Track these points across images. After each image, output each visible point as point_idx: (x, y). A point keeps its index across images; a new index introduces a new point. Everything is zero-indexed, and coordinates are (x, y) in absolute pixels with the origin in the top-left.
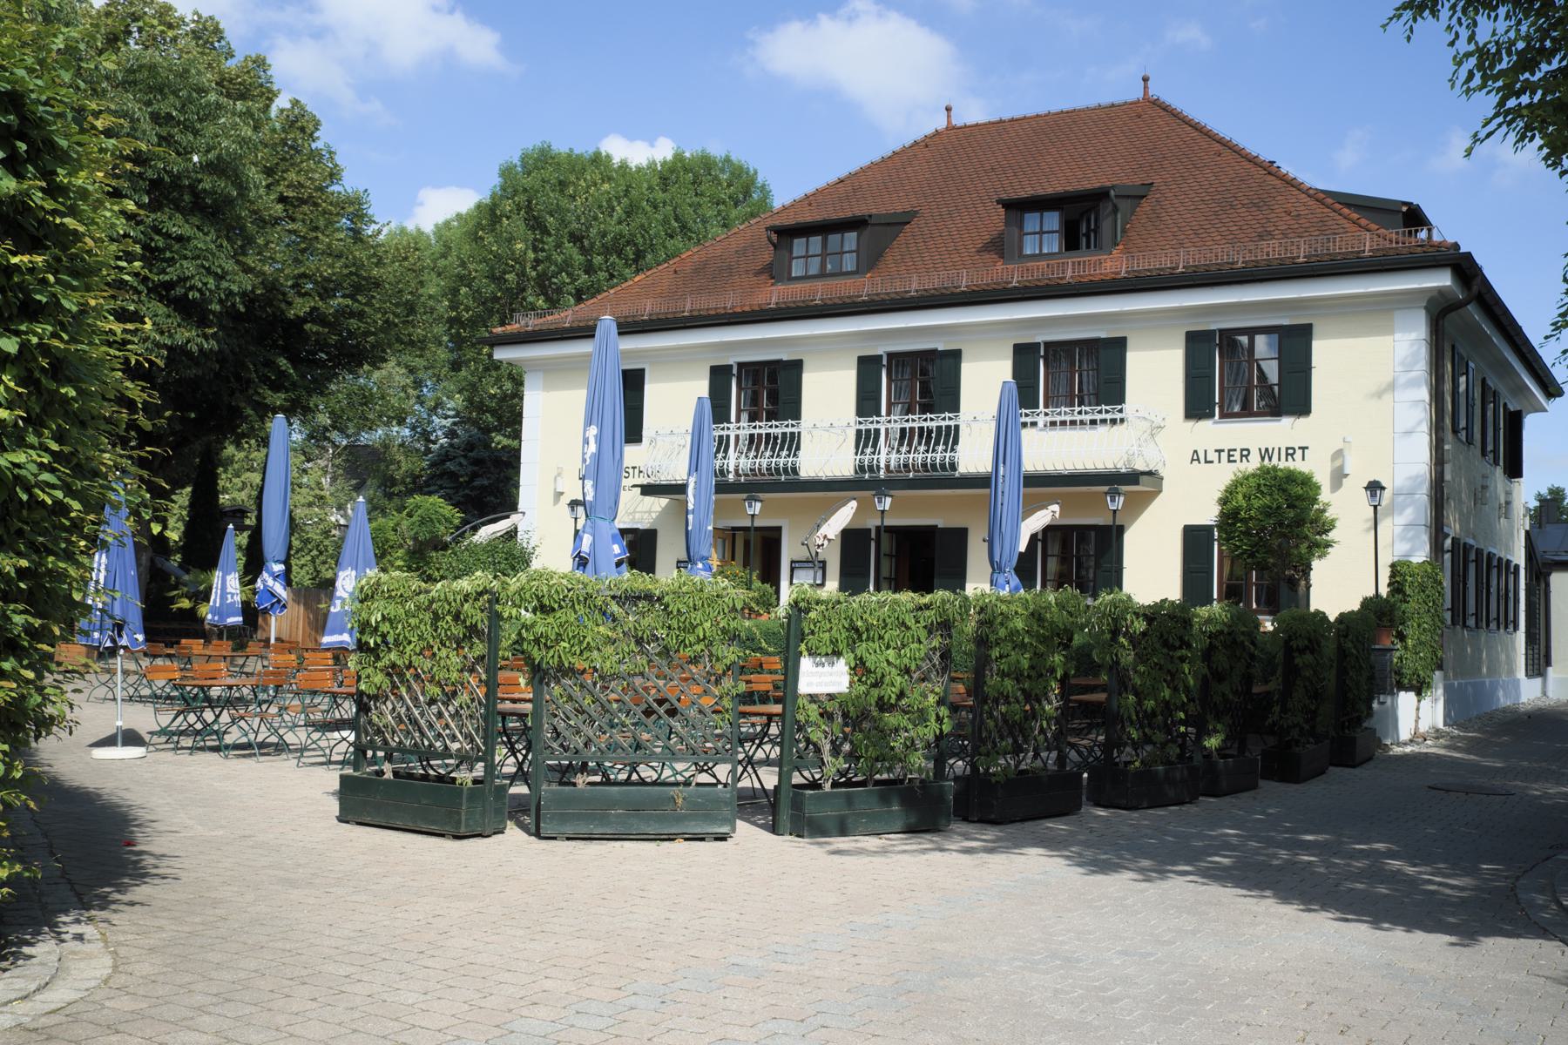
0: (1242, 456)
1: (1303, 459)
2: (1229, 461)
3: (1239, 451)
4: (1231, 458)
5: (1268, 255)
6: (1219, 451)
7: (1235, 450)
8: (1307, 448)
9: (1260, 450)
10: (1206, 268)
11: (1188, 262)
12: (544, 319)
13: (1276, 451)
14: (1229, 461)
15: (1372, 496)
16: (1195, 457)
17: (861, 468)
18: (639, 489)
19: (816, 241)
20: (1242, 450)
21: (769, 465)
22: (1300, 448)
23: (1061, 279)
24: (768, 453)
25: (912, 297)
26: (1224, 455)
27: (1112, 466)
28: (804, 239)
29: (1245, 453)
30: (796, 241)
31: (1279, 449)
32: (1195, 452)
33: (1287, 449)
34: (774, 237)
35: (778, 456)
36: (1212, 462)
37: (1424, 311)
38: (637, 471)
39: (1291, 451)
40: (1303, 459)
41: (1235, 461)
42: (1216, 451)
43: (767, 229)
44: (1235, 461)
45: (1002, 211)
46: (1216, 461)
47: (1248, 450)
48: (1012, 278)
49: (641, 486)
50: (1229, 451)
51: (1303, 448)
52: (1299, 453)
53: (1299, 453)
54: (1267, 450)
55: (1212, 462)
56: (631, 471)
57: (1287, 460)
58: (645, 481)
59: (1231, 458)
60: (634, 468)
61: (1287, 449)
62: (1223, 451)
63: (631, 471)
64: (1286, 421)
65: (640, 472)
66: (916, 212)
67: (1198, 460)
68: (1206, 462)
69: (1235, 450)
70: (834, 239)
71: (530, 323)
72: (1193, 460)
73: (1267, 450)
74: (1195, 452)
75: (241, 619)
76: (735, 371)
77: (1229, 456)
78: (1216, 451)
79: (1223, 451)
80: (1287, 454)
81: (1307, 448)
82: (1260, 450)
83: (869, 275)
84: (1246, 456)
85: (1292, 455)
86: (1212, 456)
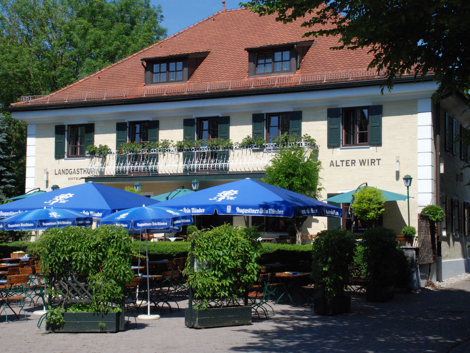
0: (352, 163)
1: (379, 164)
2: (347, 165)
3: (351, 161)
4: (347, 164)
5: (363, 75)
6: (342, 161)
7: (349, 161)
8: (380, 159)
9: (360, 160)
10: (336, 81)
11: (328, 78)
12: (36, 99)
13: (367, 161)
14: (347, 165)
15: (406, 182)
16: (332, 164)
17: (185, 170)
18: (84, 179)
19: (164, 66)
20: (352, 161)
21: (144, 168)
22: (377, 159)
23: (273, 85)
24: (122, 164)
25: (207, 93)
26: (344, 163)
27: (248, 170)
28: (175, 63)
29: (353, 162)
30: (155, 66)
31: (368, 160)
32: (332, 161)
33: (372, 160)
34: (145, 64)
35: (202, 162)
36: (339, 166)
37: (430, 99)
38: (83, 171)
39: (373, 161)
40: (379, 164)
41: (349, 165)
42: (341, 161)
43: (141, 60)
44: (349, 165)
45: (247, 54)
46: (341, 165)
47: (354, 160)
48: (252, 84)
49: (86, 178)
50: (347, 161)
51: (379, 160)
52: (377, 162)
53: (377, 162)
54: (363, 160)
55: (339, 166)
56: (80, 171)
57: (371, 165)
58: (87, 175)
59: (347, 164)
60: (81, 169)
61: (372, 160)
62: (344, 161)
63: (80, 171)
64: (372, 149)
65: (84, 171)
66: (209, 52)
67: (333, 165)
68: (337, 166)
69: (349, 161)
70: (172, 65)
71: (30, 101)
72: (331, 165)
73: (363, 160)
74: (332, 161)
75: (442, 261)
76: (128, 125)
77: (347, 163)
78: (341, 161)
79: (344, 161)
80: (372, 162)
81: (380, 159)
82: (360, 160)
83: (188, 82)
84: (354, 163)
85: (374, 162)
86: (339, 163)
